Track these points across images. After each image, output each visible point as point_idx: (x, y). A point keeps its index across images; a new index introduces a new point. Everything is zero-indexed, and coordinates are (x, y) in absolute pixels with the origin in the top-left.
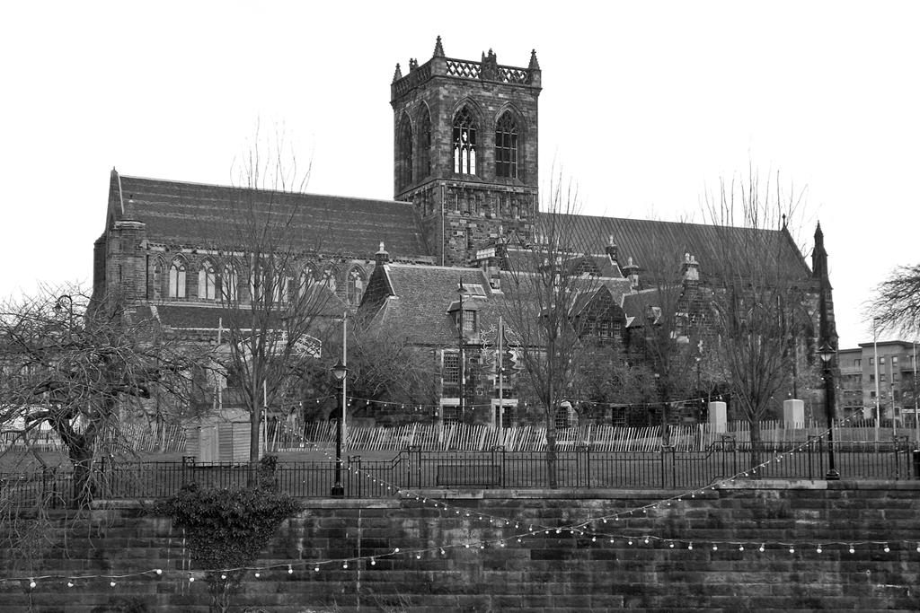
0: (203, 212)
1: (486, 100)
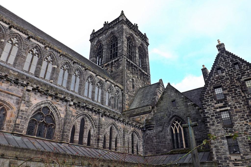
1: (136, 38)
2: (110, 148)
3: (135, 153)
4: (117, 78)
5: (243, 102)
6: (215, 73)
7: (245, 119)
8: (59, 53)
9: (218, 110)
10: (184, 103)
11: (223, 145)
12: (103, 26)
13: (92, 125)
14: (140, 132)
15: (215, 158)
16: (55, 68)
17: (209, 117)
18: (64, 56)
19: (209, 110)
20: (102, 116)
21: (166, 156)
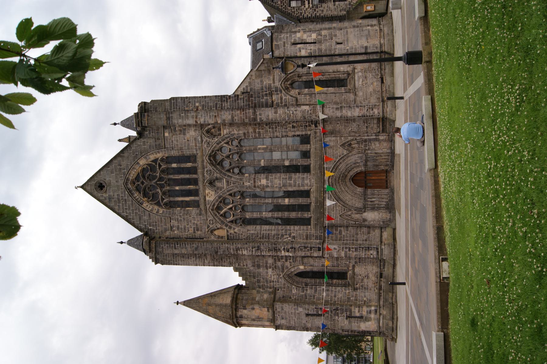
9: (311, 5)
11: (339, 5)
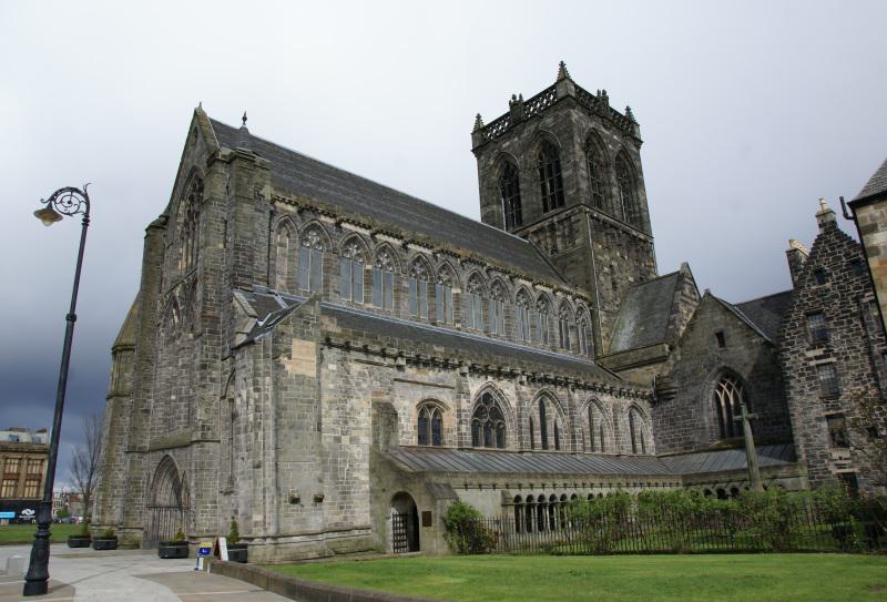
0: (326, 186)
1: (607, 137)
2: (593, 449)
3: (640, 453)
4: (572, 269)
5: (862, 348)
6: (809, 281)
7: (864, 383)
8: (459, 256)
9: (812, 363)
10: (745, 341)
12: (507, 109)
13: (559, 410)
14: (645, 405)
15: (804, 456)
16: (457, 294)
17: (794, 378)
18: (470, 260)
19: (794, 362)
20: (573, 390)
21: (705, 454)
